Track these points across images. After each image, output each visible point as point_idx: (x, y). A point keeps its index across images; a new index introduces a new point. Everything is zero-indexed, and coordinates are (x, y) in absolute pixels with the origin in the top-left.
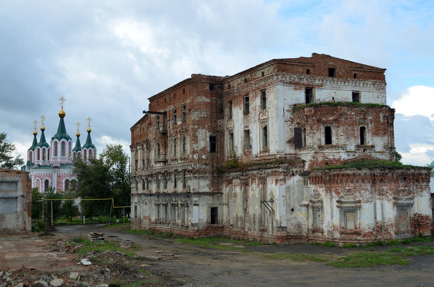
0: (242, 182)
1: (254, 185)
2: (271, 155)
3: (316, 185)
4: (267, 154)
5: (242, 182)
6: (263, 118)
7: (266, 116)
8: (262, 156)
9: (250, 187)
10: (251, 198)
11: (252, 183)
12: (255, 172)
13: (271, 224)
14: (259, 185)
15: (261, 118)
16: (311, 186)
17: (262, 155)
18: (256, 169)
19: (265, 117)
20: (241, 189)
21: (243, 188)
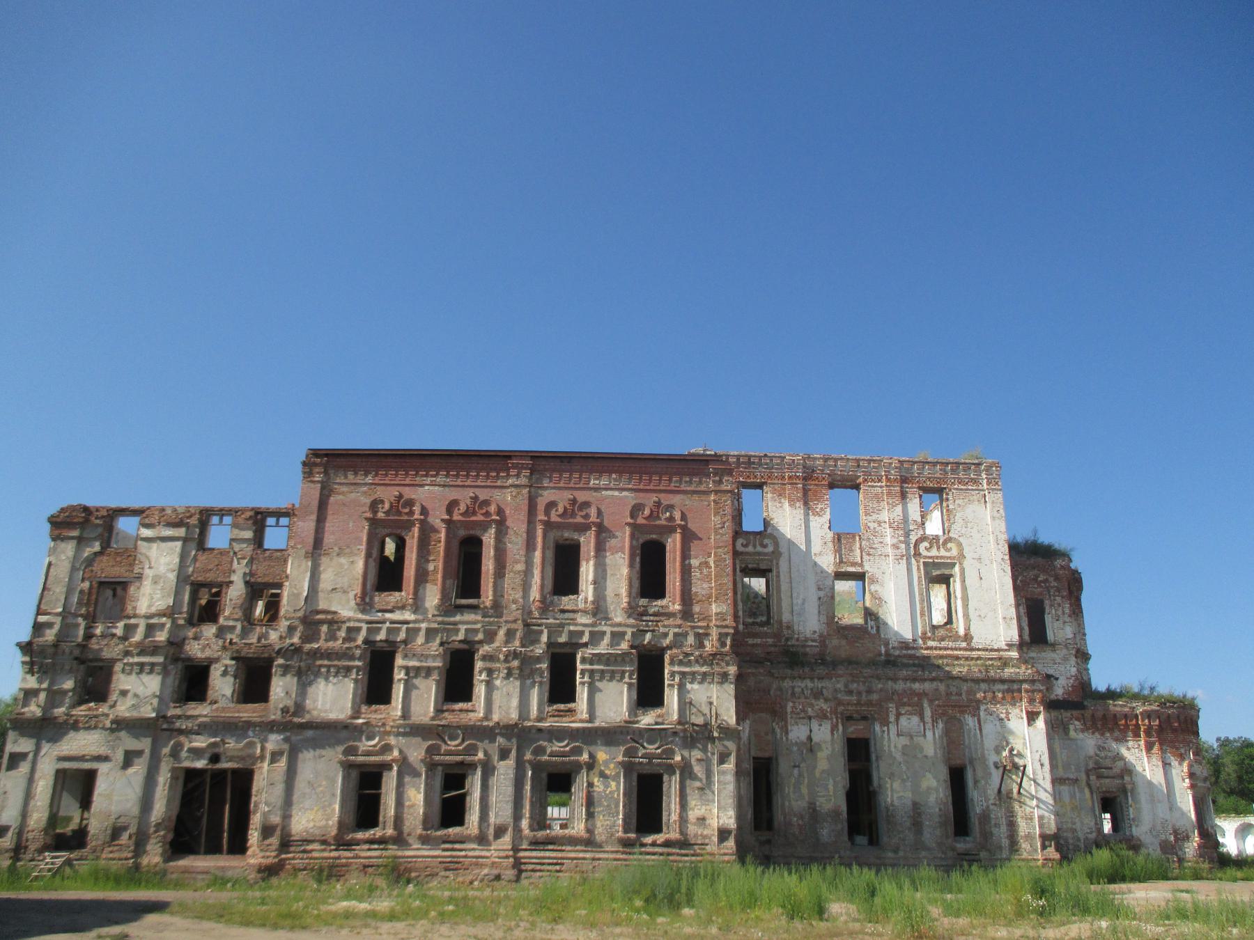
0: (841, 708)
1: (910, 722)
2: (979, 650)
3: (1102, 734)
4: (964, 645)
5: (841, 708)
6: (934, 552)
7: (949, 550)
8: (936, 648)
9: (893, 728)
10: (899, 756)
11: (898, 715)
12: (927, 686)
13: (1004, 828)
14: (934, 721)
15: (924, 553)
16: (1081, 736)
17: (931, 643)
18: (933, 680)
19: (943, 553)
20: (834, 728)
21: (841, 728)
